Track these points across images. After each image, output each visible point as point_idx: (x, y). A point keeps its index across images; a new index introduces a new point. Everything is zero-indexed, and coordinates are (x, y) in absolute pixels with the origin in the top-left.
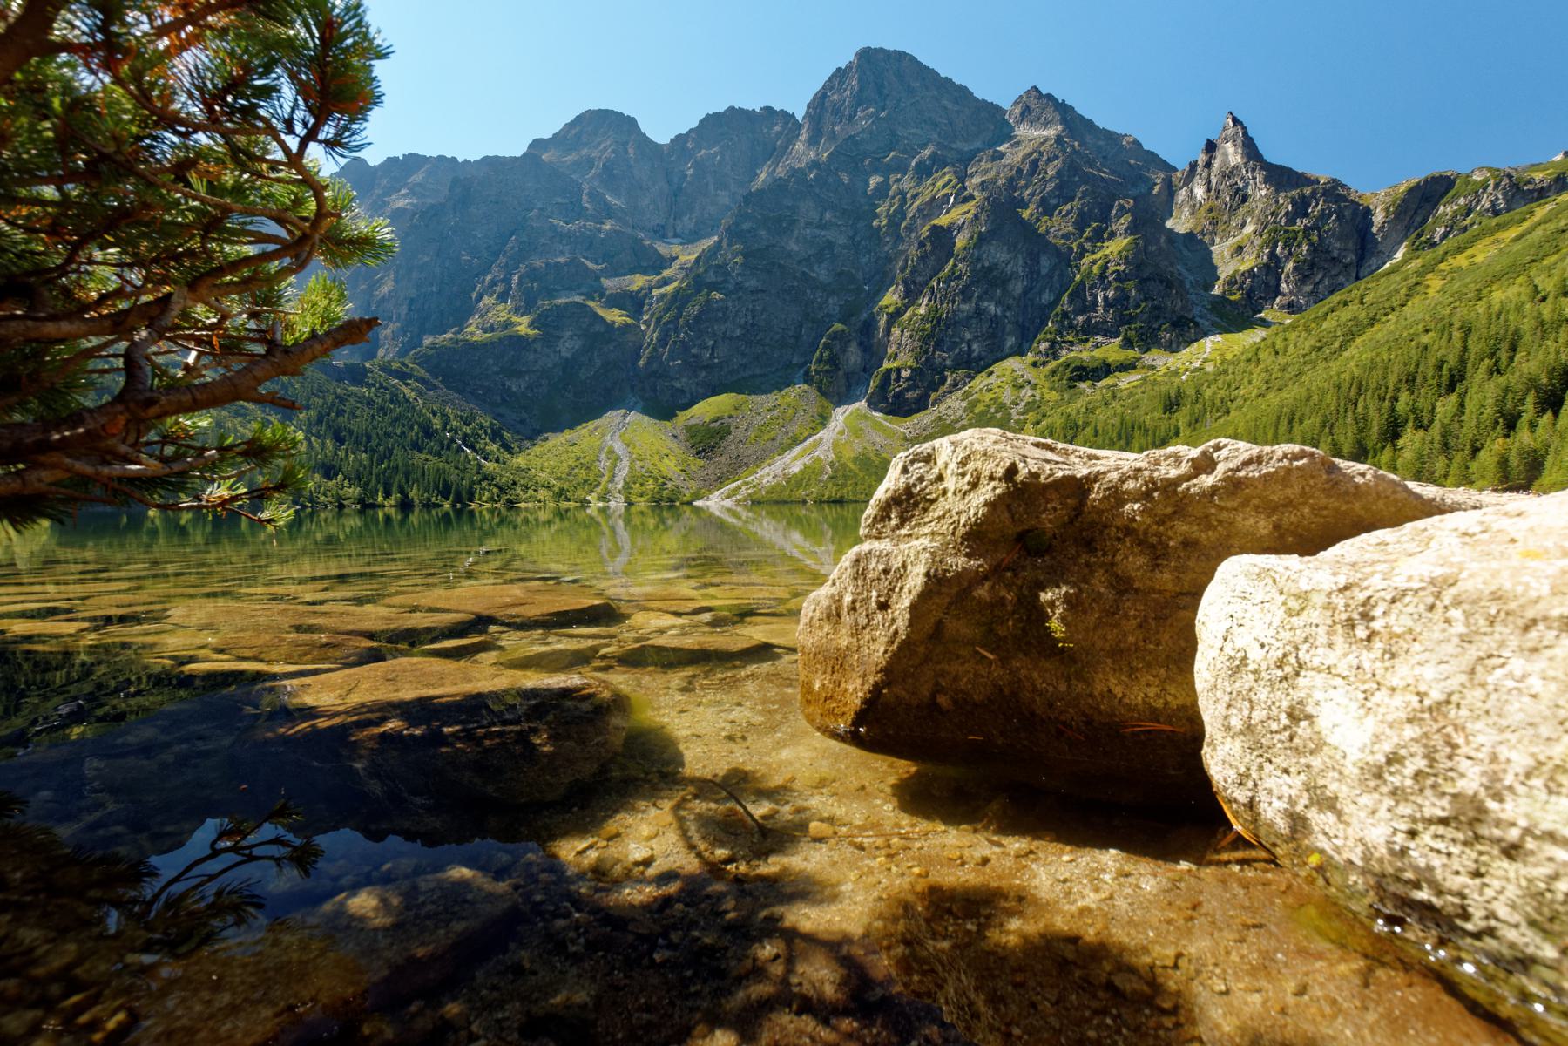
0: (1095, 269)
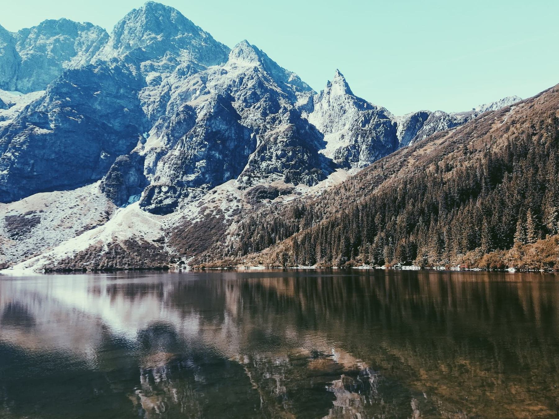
0: (272, 139)
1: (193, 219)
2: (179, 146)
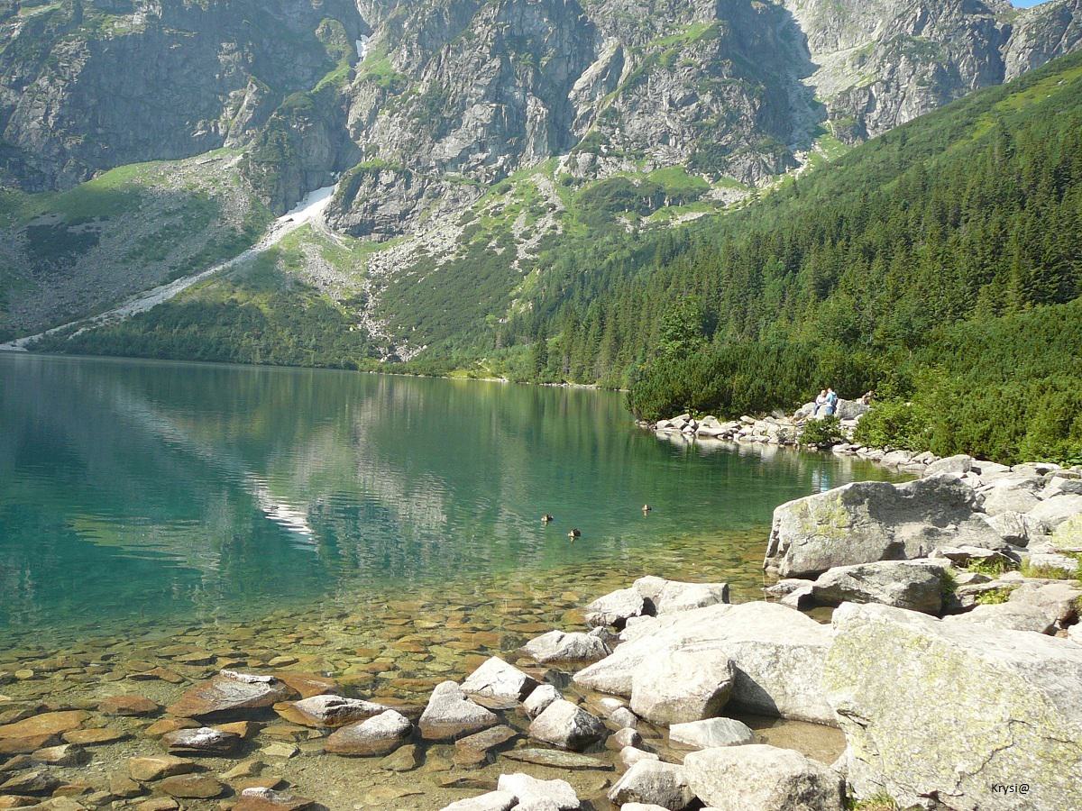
0: (663, 59)
2: (429, 73)
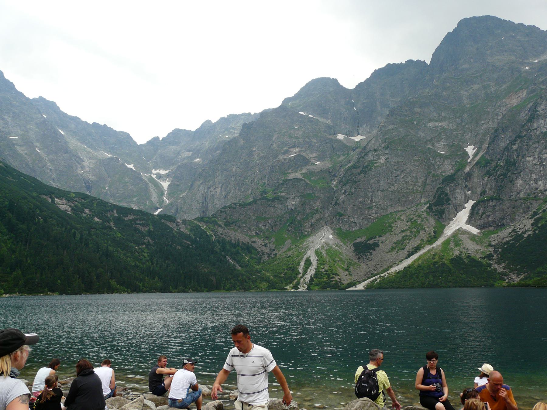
1: (525, 233)
